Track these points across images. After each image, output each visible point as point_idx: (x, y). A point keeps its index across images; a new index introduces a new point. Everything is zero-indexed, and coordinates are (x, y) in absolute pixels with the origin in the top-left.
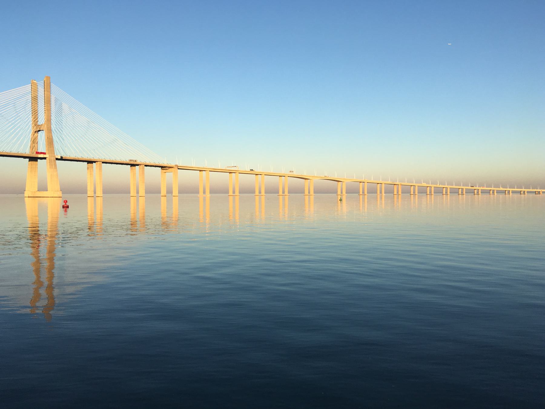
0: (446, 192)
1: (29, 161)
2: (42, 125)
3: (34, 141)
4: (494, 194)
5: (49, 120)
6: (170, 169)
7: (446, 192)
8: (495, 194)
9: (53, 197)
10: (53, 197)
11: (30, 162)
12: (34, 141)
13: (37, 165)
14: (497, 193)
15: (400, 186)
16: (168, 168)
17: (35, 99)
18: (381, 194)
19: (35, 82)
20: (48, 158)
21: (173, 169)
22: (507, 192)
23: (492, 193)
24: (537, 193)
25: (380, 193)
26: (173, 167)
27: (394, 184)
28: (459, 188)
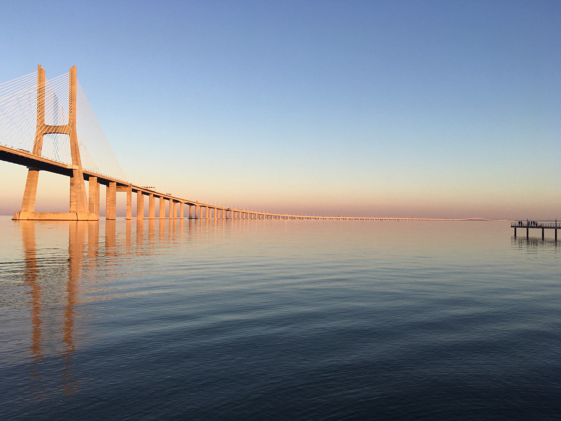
0: (247, 217)
1: (29, 171)
2: (60, 126)
3: (38, 146)
4: (272, 219)
5: (72, 123)
6: (123, 188)
7: (247, 217)
8: (272, 218)
9: (87, 220)
10: (87, 220)
11: (29, 171)
12: (38, 146)
13: (37, 177)
14: (273, 218)
15: (224, 210)
16: (122, 186)
17: (41, 91)
18: (213, 218)
19: (42, 68)
20: (77, 171)
21: (128, 188)
22: (277, 217)
23: (270, 218)
24: (293, 218)
25: (212, 217)
26: (127, 186)
27: (219, 209)
28: (252, 214)
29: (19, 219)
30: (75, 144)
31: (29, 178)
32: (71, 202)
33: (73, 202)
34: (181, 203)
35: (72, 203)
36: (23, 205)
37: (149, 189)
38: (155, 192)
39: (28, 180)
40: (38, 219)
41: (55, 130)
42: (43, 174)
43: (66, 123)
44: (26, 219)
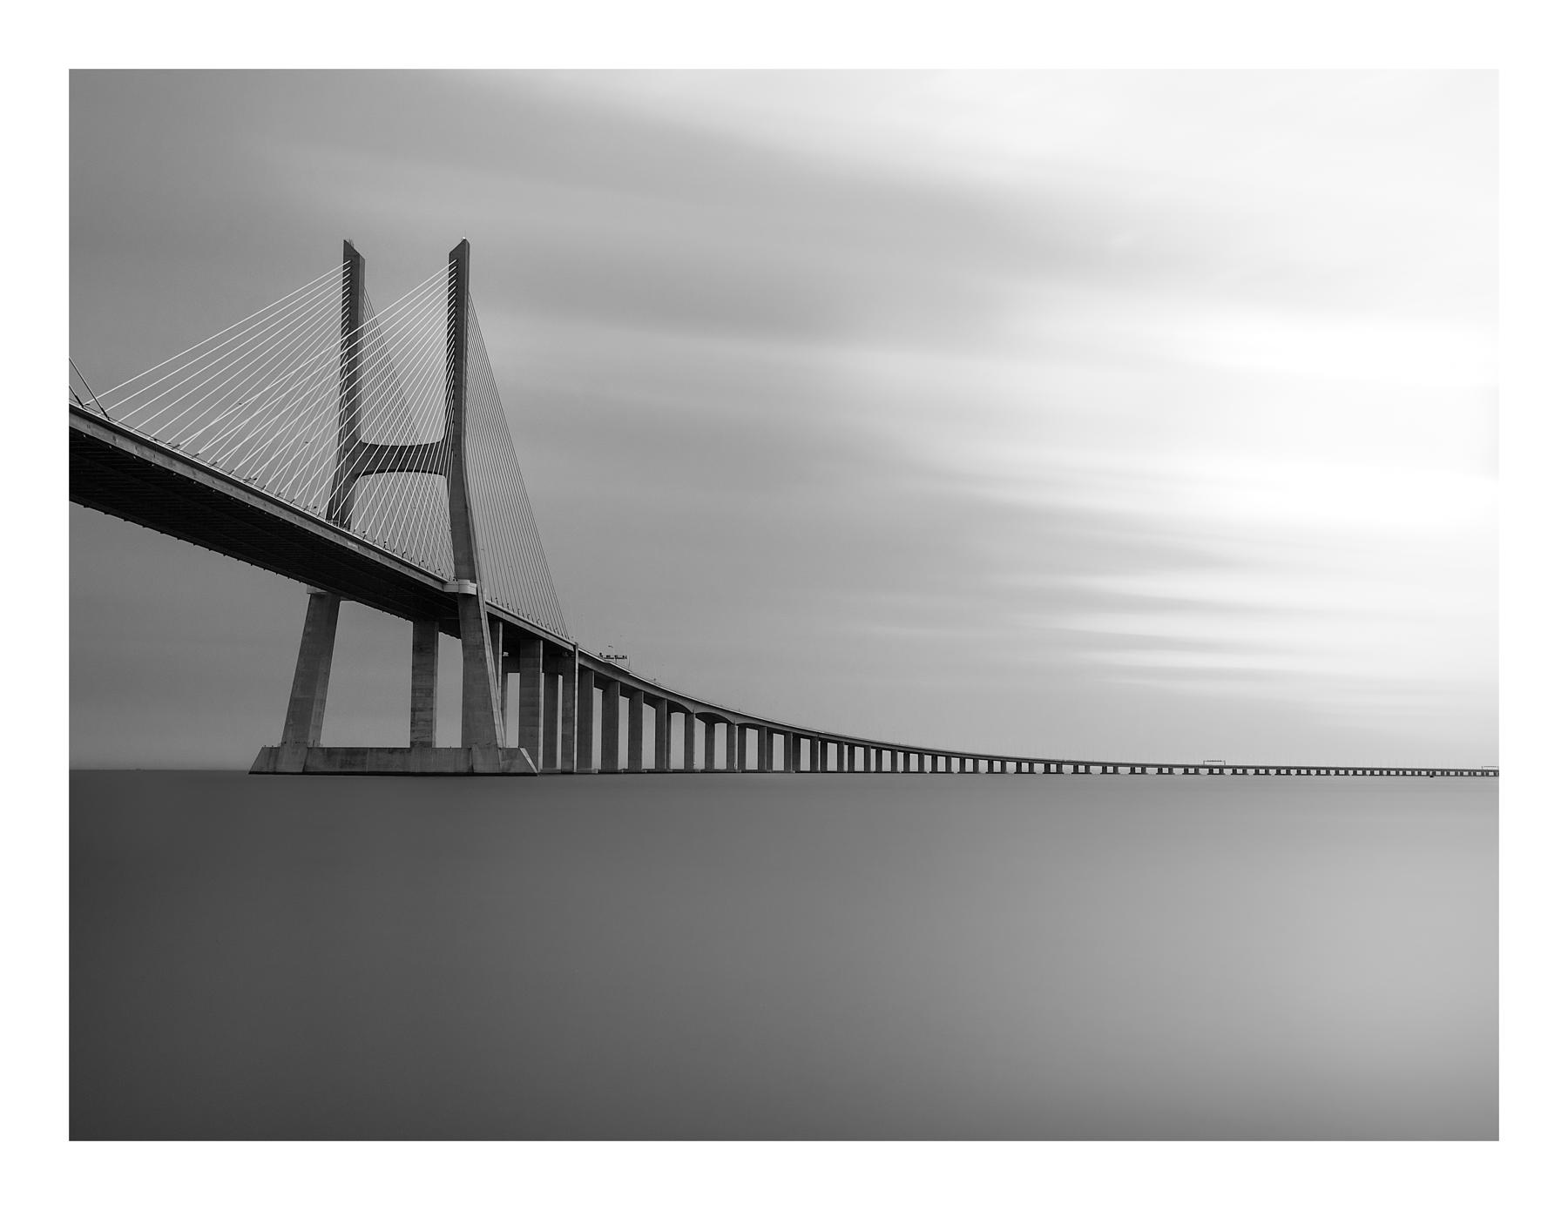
29: (277, 771)
30: (466, 507)
31: (310, 630)
32: (413, 710)
33: (421, 710)
34: (688, 714)
35: (417, 713)
36: (291, 723)
37: (613, 662)
38: (625, 674)
39: (306, 634)
40: (338, 770)
41: (402, 459)
42: (353, 615)
43: (432, 431)
44: (301, 771)
